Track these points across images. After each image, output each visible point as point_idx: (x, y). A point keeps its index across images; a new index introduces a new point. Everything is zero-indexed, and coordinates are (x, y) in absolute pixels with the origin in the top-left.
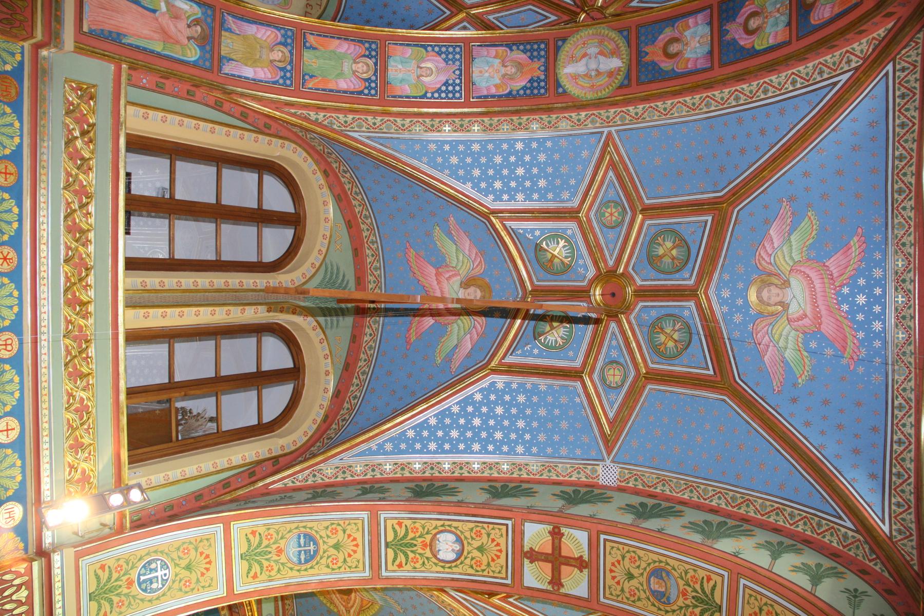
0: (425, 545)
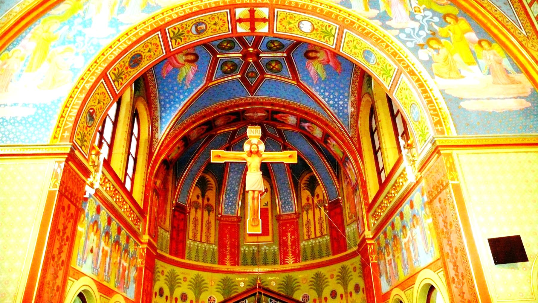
0: (317, 30)
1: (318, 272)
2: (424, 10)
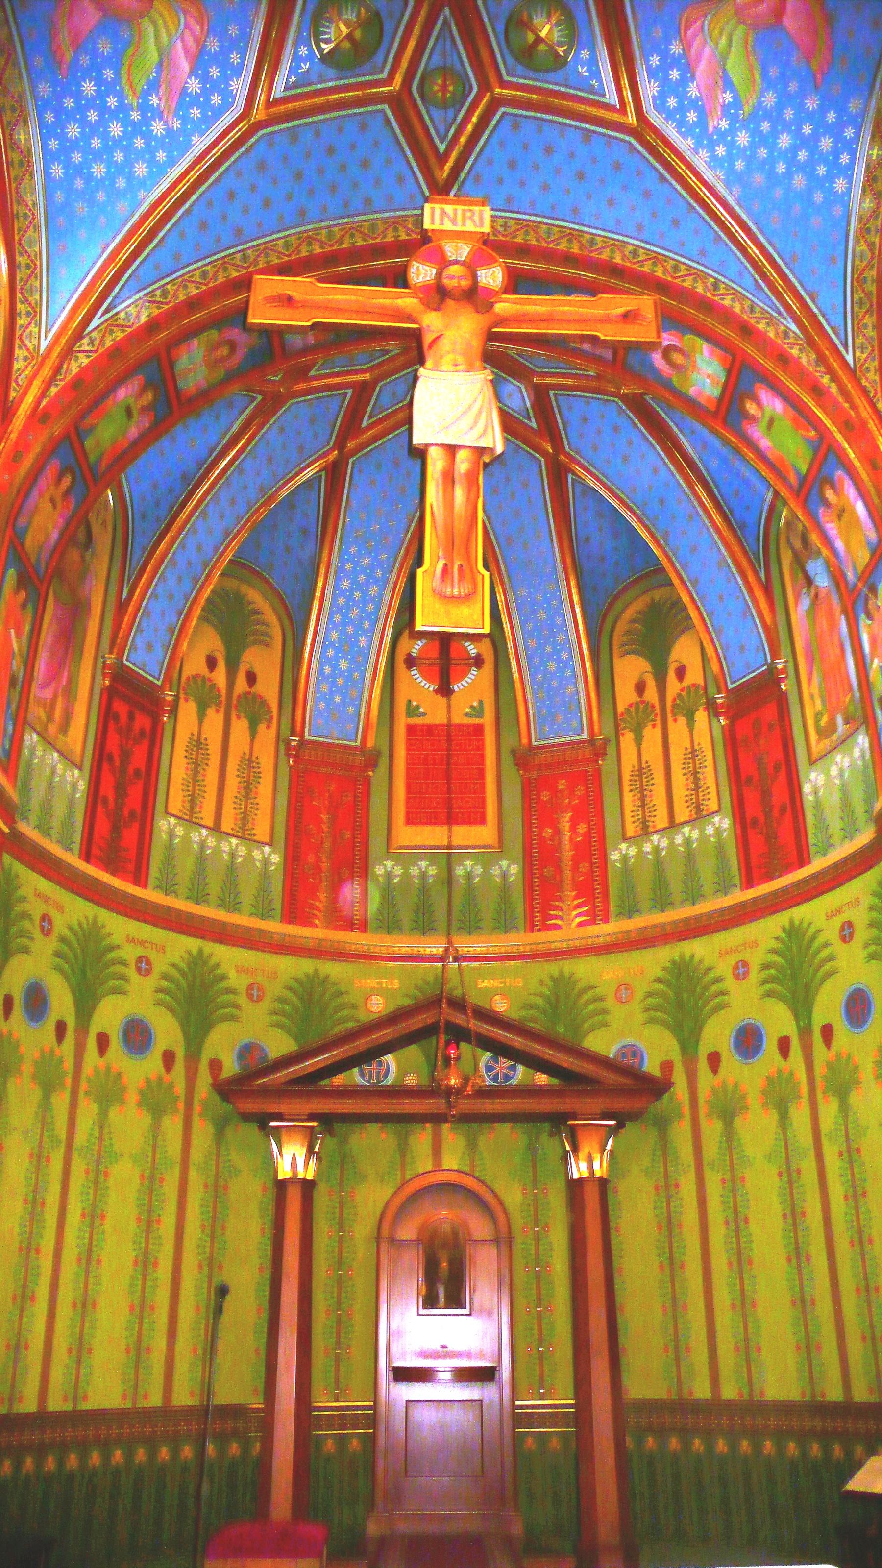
1: (682, 956)
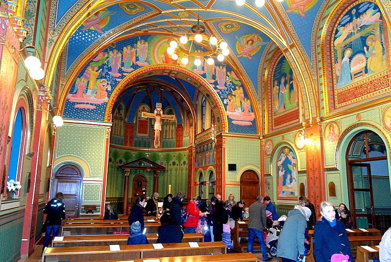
2: (230, 82)
